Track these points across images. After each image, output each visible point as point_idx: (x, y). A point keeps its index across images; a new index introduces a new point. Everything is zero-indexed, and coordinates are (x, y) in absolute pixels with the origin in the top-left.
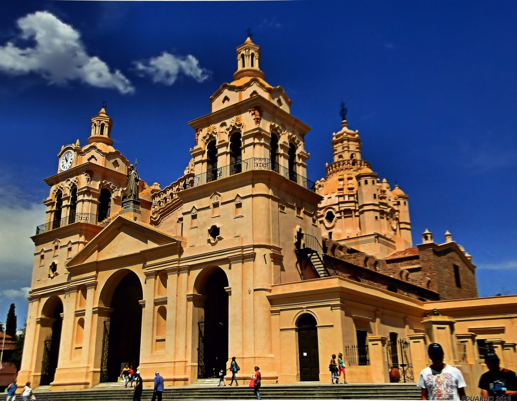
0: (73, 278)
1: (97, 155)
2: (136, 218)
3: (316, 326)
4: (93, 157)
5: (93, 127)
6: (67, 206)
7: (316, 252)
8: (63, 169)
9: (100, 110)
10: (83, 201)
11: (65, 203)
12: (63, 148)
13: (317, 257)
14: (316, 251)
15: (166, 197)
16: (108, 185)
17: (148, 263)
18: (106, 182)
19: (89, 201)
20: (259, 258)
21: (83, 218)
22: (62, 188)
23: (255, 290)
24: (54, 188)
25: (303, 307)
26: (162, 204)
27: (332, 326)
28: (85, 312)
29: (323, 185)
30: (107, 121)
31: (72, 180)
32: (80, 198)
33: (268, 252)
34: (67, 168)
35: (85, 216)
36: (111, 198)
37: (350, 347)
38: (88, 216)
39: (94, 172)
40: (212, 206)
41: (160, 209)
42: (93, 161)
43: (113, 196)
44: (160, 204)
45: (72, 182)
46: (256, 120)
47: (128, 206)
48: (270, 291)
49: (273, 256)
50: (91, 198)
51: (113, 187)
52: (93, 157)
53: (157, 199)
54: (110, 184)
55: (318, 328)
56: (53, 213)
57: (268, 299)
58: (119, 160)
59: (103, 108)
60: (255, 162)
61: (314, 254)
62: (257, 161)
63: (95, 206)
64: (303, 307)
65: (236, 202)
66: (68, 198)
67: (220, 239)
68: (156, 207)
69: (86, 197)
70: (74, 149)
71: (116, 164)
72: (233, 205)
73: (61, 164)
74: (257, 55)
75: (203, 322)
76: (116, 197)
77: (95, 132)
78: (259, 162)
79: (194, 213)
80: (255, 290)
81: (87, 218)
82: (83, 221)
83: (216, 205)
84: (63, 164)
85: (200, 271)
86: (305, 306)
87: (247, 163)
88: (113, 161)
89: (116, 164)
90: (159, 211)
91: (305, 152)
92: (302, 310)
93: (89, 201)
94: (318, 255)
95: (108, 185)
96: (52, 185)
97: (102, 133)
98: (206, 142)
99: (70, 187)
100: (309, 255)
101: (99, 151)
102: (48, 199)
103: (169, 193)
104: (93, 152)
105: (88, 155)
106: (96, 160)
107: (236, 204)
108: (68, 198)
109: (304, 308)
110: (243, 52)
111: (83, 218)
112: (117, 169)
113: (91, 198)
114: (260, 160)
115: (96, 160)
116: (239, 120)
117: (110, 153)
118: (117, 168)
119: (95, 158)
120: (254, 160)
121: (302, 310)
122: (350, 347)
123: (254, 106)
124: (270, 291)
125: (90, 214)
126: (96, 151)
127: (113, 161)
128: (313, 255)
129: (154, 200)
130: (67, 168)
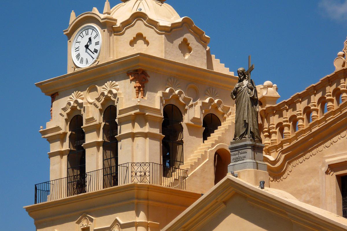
1: (149, 33)
2: (264, 183)
4: (140, 36)
6: (97, 144)
8: (78, 63)
10: (133, 136)
11: (90, 138)
12: (73, 18)
15: (294, 116)
16: (177, 97)
18: (171, 91)
19: (145, 135)
22: (81, 105)
24: (61, 103)
26: (286, 130)
31: (104, 89)
32: (125, 129)
34: (87, 62)
35: (142, 170)
36: (183, 124)
39: (148, 73)
41: (282, 143)
43: (187, 119)
44: (281, 130)
45: (103, 94)
47: (242, 155)
50: (146, 129)
51: (184, 99)
52: (140, 36)
53: (275, 120)
54: (180, 93)
56: (65, 157)
58: (190, 37)
63: (157, 146)
66: (96, 128)
68: (274, 137)
69: (137, 129)
71: (185, 47)
73: (73, 54)
76: (191, 121)
82: (137, 181)
84: (77, 53)
88: (179, 41)
89: (185, 47)
90: (281, 145)
93: (145, 135)
95: (177, 97)
96: (54, 96)
99: (99, 104)
101: (153, 24)
102: (50, 125)
103: (301, 106)
104: (140, 27)
105: (130, 34)
106: (147, 43)
108: (96, 128)
111: (139, 174)
112: (187, 59)
113: (146, 129)
115: (147, 43)
117: (175, 26)
118: (187, 57)
125: (151, 164)
127: (179, 41)
129: (268, 121)
130: (87, 62)
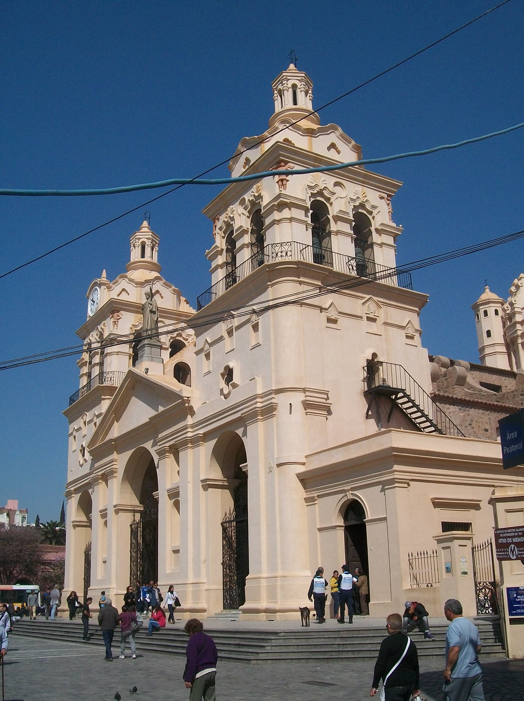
0: (96, 465)
1: (130, 287)
2: (148, 369)
3: (364, 520)
4: (124, 290)
5: (132, 249)
7: (403, 391)
9: (142, 223)
13: (406, 399)
14: (401, 389)
17: (160, 436)
20: (282, 411)
21: (109, 379)
23: (279, 465)
25: (345, 489)
27: (385, 519)
28: (107, 513)
29: (521, 284)
30: (147, 237)
33: (298, 398)
35: (109, 376)
37: (415, 554)
38: (113, 376)
40: (226, 335)
42: (124, 297)
46: (280, 183)
48: (304, 464)
49: (307, 405)
52: (124, 290)
55: (366, 524)
57: (300, 480)
59: (146, 220)
60: (273, 251)
61: (400, 395)
62: (277, 248)
64: (346, 488)
65: (252, 322)
67: (235, 386)
70: (99, 283)
72: (249, 326)
74: (302, 86)
75: (233, 521)
77: (135, 255)
78: (280, 250)
79: (206, 351)
80: (279, 465)
81: (112, 379)
83: (230, 333)
85: (214, 441)
86: (349, 487)
87: (269, 256)
91: (394, 225)
92: (344, 494)
94: (408, 396)
97: (143, 256)
98: (224, 236)
100: (393, 397)
107: (252, 326)
109: (348, 490)
110: (280, 87)
114: (281, 245)
116: (260, 190)
119: (126, 291)
120: (272, 247)
121: (344, 494)
122: (415, 554)
123: (276, 161)
124: (304, 464)
125: (115, 372)
126: (127, 282)
128: (398, 397)
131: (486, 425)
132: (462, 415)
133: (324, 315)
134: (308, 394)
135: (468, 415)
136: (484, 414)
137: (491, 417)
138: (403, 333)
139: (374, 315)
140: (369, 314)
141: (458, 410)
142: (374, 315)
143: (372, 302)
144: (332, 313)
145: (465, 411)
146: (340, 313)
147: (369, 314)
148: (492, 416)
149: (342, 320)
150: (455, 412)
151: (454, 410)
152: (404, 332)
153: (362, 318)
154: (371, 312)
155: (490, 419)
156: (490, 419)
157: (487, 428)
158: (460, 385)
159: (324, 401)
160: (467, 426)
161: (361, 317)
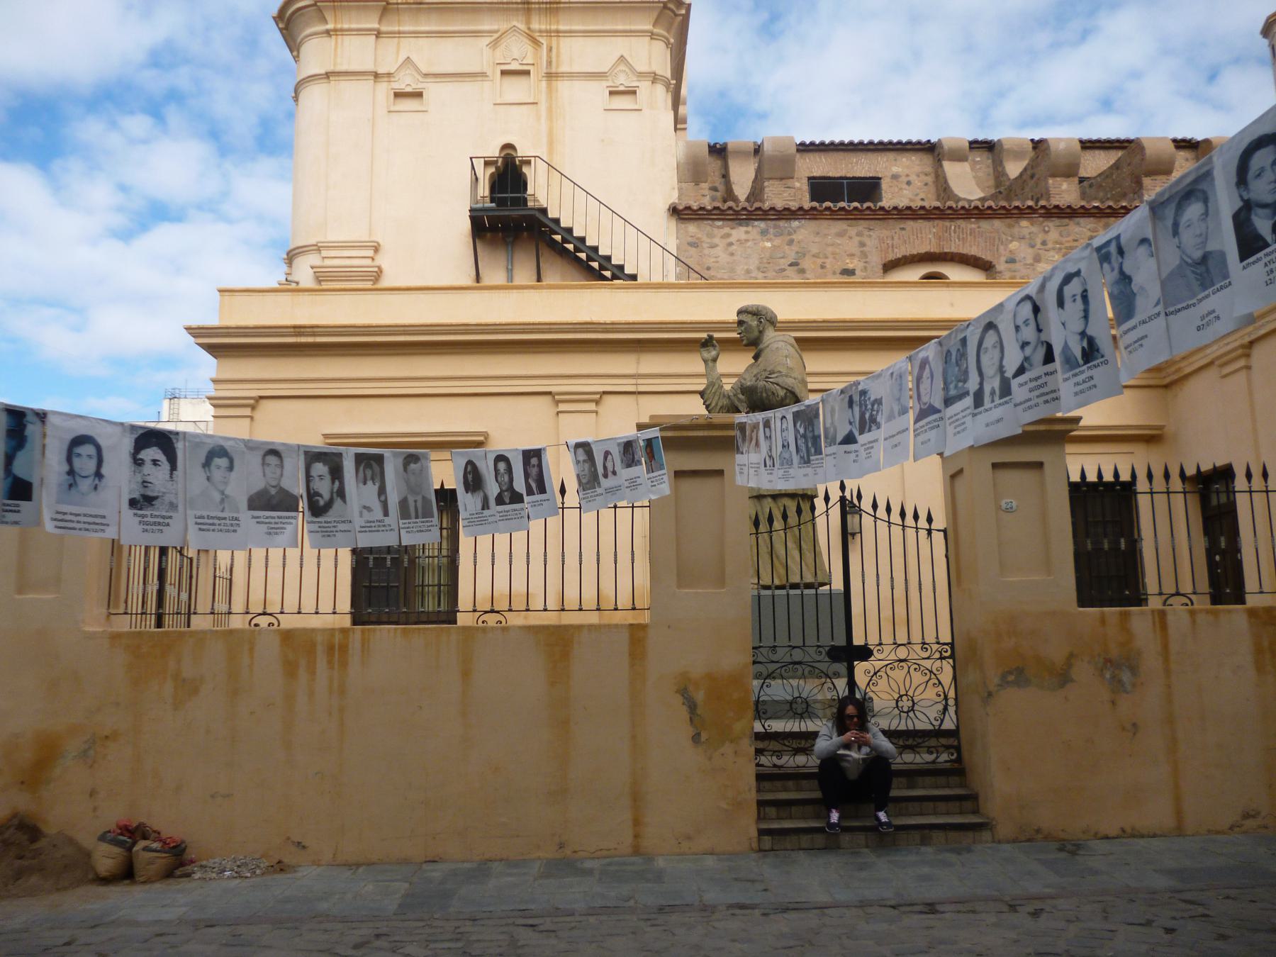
131: (848, 261)
132: (768, 244)
133: (384, 89)
134: (324, 253)
135: (791, 242)
136: (841, 234)
137: (865, 239)
138: (601, 88)
139: (521, 64)
140: (510, 63)
141: (758, 237)
142: (521, 64)
143: (517, 35)
144: (406, 82)
145: (782, 235)
146: (426, 75)
147: (510, 63)
148: (870, 236)
149: (433, 91)
150: (747, 241)
151: (743, 237)
152: (605, 84)
153: (487, 76)
154: (514, 59)
155: (862, 244)
156: (862, 244)
157: (851, 266)
158: (781, 179)
159: (368, 262)
160: (784, 270)
161: (482, 75)
